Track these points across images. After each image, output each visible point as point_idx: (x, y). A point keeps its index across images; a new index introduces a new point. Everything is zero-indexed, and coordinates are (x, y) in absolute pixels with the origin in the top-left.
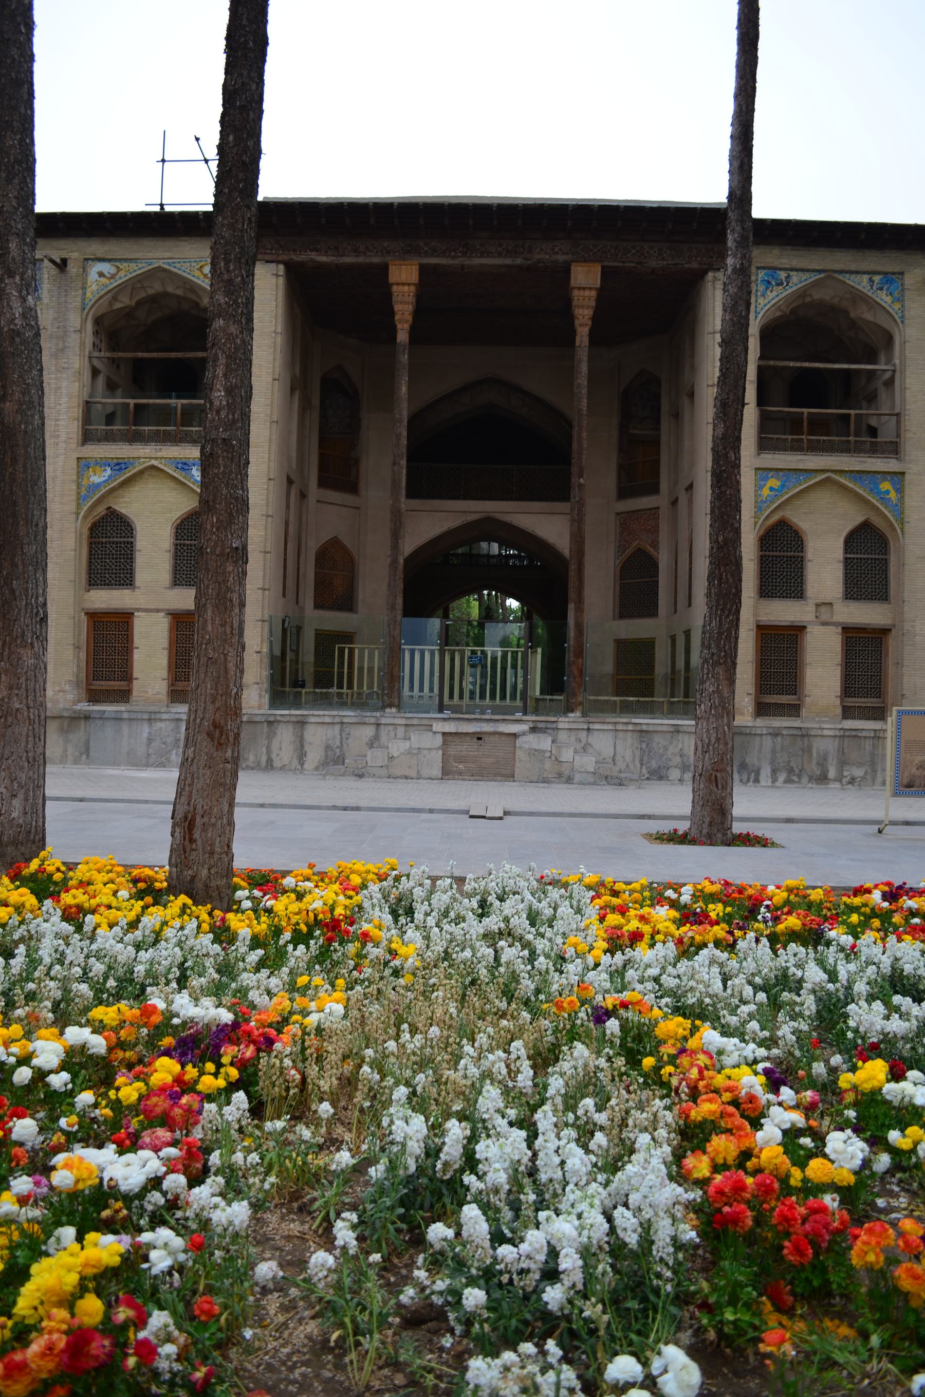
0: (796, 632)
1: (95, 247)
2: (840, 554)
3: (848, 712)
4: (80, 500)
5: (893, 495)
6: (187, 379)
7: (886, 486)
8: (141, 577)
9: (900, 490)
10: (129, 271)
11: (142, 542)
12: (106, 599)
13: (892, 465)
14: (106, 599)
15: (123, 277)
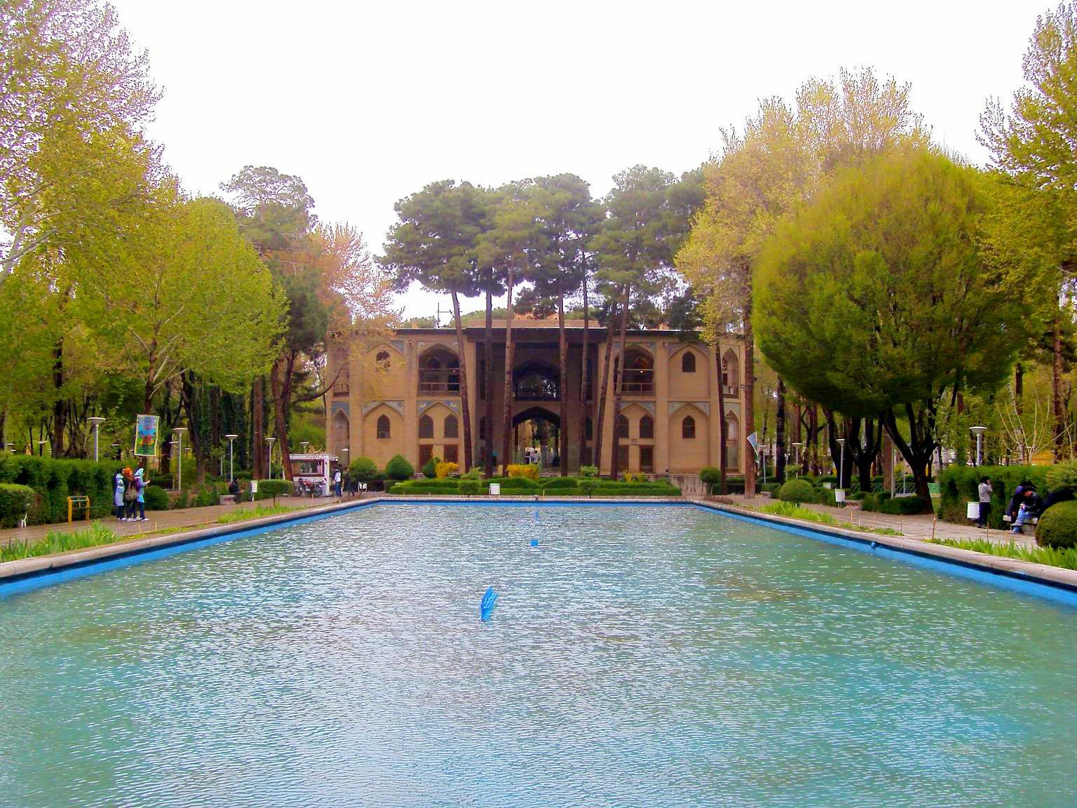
0: (626, 448)
1: (420, 337)
2: (638, 425)
3: (641, 470)
4: (417, 413)
5: (653, 408)
6: (456, 388)
7: (651, 405)
8: (435, 435)
9: (655, 406)
10: (429, 345)
11: (435, 425)
12: (425, 441)
13: (652, 399)
14: (425, 441)
15: (428, 346)
